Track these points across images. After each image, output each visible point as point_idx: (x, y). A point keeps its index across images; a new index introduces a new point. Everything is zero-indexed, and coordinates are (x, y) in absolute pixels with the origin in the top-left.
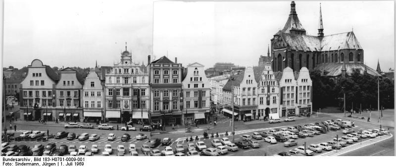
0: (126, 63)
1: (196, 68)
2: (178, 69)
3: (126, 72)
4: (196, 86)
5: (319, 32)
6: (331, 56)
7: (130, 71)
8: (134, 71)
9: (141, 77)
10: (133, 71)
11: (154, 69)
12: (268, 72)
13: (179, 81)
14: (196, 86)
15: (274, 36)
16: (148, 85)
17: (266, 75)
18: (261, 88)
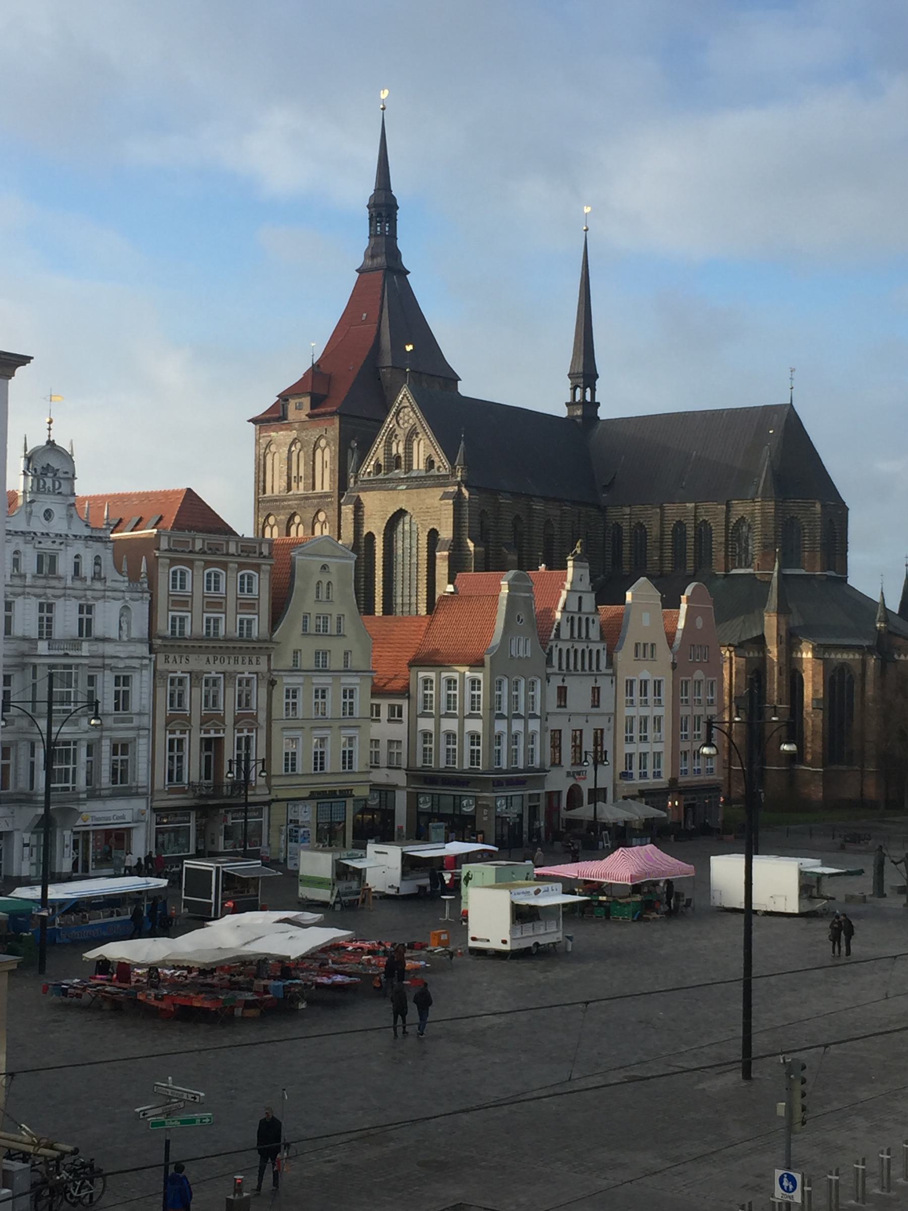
0: (48, 515)
1: (324, 567)
2: (257, 567)
3: (45, 569)
4: (321, 655)
5: (574, 389)
6: (668, 538)
7: (64, 566)
8: (87, 569)
9: (119, 605)
10: (77, 566)
11: (173, 562)
12: (580, 598)
13: (259, 626)
14: (321, 655)
15: (284, 397)
16: (144, 650)
17: (572, 618)
18: (556, 682)
